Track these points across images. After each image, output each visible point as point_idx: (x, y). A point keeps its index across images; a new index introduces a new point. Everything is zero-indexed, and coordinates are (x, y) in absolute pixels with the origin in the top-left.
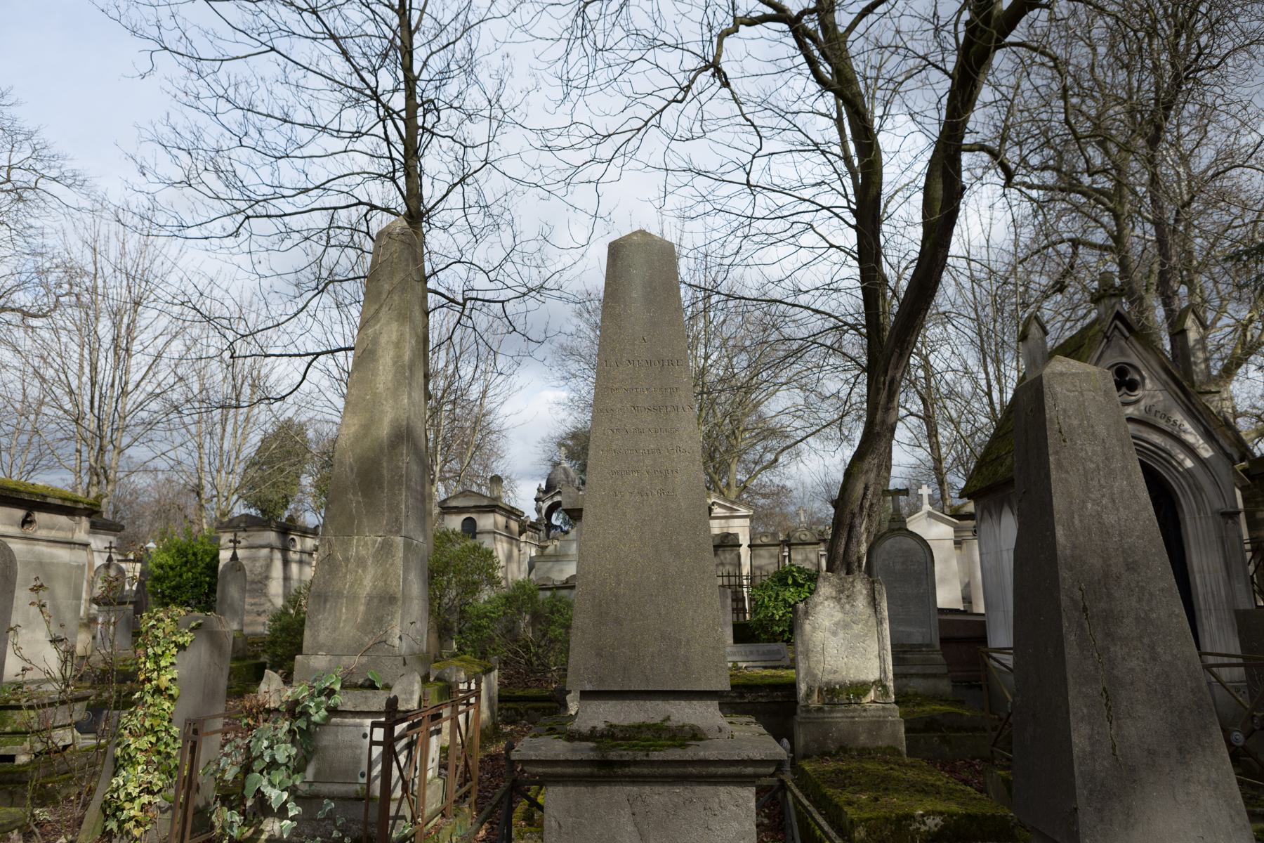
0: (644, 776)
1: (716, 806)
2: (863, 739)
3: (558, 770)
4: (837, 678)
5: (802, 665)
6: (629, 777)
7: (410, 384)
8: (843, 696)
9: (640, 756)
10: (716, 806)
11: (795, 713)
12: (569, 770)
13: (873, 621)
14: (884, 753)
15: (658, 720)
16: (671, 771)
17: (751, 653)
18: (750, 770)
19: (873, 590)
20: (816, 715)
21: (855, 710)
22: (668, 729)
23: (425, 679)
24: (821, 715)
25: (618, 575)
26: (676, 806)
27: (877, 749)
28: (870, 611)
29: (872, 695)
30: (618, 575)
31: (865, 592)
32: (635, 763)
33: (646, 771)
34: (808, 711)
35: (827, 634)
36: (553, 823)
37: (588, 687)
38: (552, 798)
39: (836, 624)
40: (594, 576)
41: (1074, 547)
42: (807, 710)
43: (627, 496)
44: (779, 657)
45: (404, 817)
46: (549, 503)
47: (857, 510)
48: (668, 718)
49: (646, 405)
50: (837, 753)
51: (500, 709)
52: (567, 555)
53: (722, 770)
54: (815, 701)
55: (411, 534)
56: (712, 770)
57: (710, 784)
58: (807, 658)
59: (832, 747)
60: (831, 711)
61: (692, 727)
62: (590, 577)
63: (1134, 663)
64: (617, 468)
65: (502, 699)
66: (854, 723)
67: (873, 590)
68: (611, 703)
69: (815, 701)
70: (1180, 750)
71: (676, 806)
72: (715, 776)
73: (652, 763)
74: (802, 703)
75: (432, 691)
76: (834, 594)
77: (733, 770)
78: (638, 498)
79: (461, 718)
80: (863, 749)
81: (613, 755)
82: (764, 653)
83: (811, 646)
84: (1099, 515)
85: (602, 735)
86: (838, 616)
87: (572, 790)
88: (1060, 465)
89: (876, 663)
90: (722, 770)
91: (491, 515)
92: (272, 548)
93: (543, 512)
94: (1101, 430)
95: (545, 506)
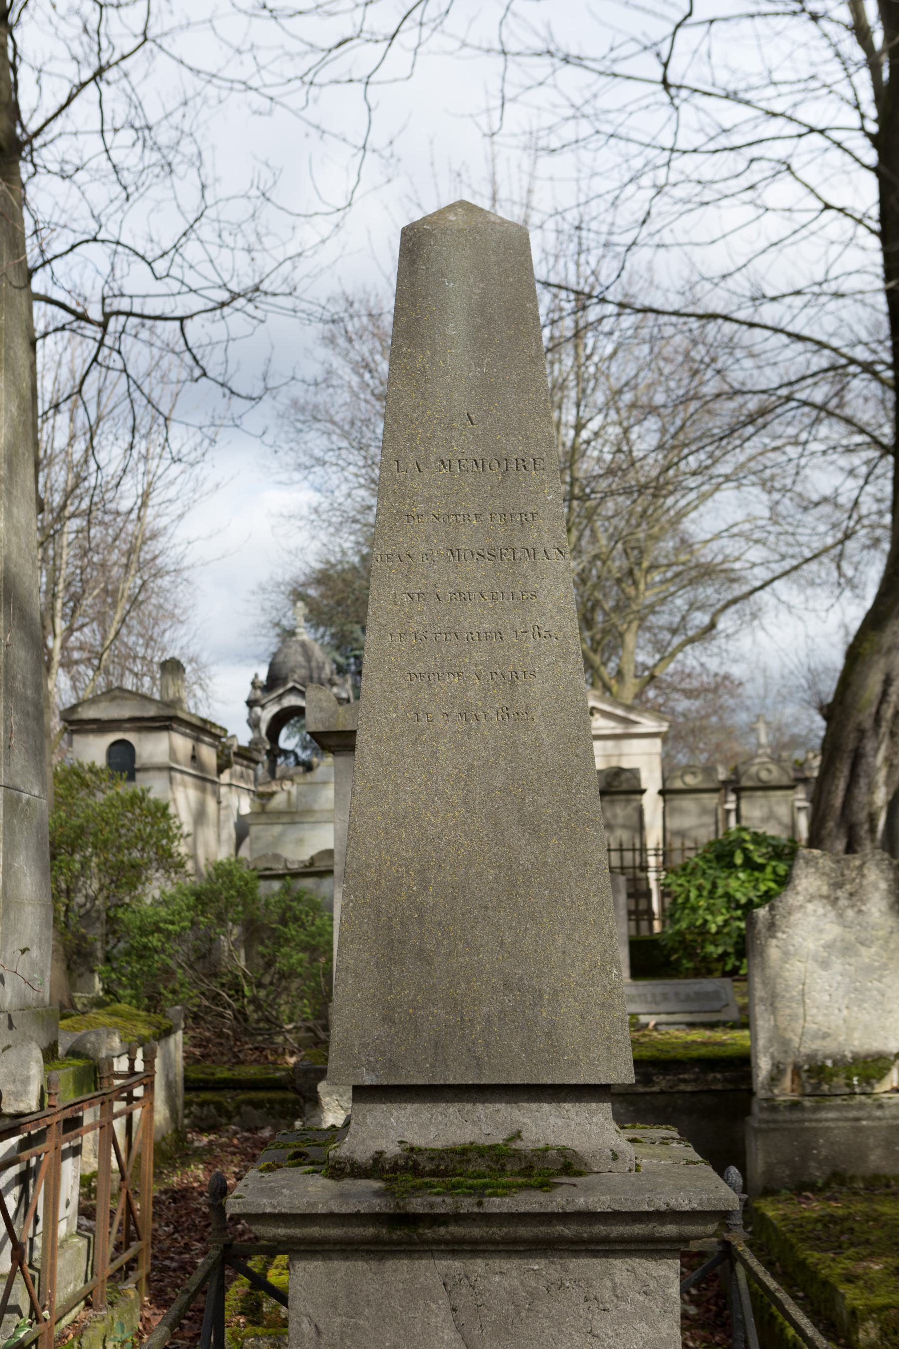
0: (474, 1242)
1: (607, 1294)
2: (876, 1160)
3: (315, 1231)
4: (829, 1046)
5: (763, 1022)
6: (446, 1242)
7: (9, 492)
8: (840, 1080)
9: (467, 1205)
10: (607, 1294)
11: (748, 1111)
12: (335, 1232)
15: (499, 1138)
16: (524, 1231)
17: (665, 997)
18: (670, 1229)
20: (787, 1116)
21: (861, 1106)
22: (517, 1155)
23: (50, 1054)
24: (797, 1115)
25: (422, 871)
26: (533, 1295)
30: (422, 871)
31: (883, 886)
32: (457, 1218)
33: (477, 1232)
35: (811, 965)
36: (306, 1327)
37: (368, 1079)
38: (304, 1281)
39: (828, 947)
40: (378, 871)
42: (772, 1106)
43: (440, 721)
44: (717, 1005)
45: (16, 1309)
46: (272, 710)
47: (868, 724)
48: (518, 1135)
49: (475, 547)
50: (827, 1185)
51: (187, 1104)
52: (309, 812)
53: (618, 1230)
54: (785, 1091)
55: (18, 782)
56: (600, 1229)
57: (595, 1254)
58: (773, 1009)
59: (818, 1174)
60: (816, 1109)
61: (562, 1151)
62: (371, 875)
64: (420, 667)
65: (191, 1085)
66: (859, 1130)
68: (410, 1108)
69: (785, 1091)
71: (533, 1295)
72: (606, 1240)
74: (761, 1093)
75: (65, 1075)
76: (825, 890)
77: (639, 1229)
78: (461, 724)
79: (119, 1125)
80: (876, 1177)
81: (416, 1205)
82: (688, 999)
83: (779, 988)
85: (395, 1167)
86: (833, 931)
87: (341, 1267)
90: (618, 1230)
93: (263, 727)
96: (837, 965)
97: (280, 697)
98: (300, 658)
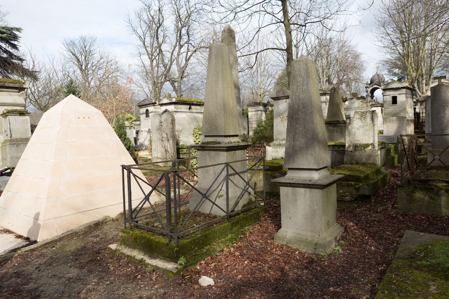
2: (364, 160)
4: (359, 142)
13: (372, 125)
14: (371, 165)
19: (372, 116)
21: (362, 152)
27: (368, 163)
28: (371, 122)
29: (370, 148)
31: (370, 116)
34: (348, 152)
35: (356, 129)
39: (359, 126)
41: (292, 103)
44: (393, 140)
46: (371, 88)
52: (351, 108)
54: (351, 148)
59: (354, 162)
63: (301, 129)
67: (372, 116)
69: (351, 148)
70: (307, 147)
73: (208, 147)
84: (299, 95)
86: (360, 124)
88: (292, 84)
89: (372, 138)
91: (325, 96)
92: (261, 111)
93: (369, 92)
94: (303, 74)
95: (369, 90)
96: (361, 129)
97: (373, 86)
98: (377, 77)
